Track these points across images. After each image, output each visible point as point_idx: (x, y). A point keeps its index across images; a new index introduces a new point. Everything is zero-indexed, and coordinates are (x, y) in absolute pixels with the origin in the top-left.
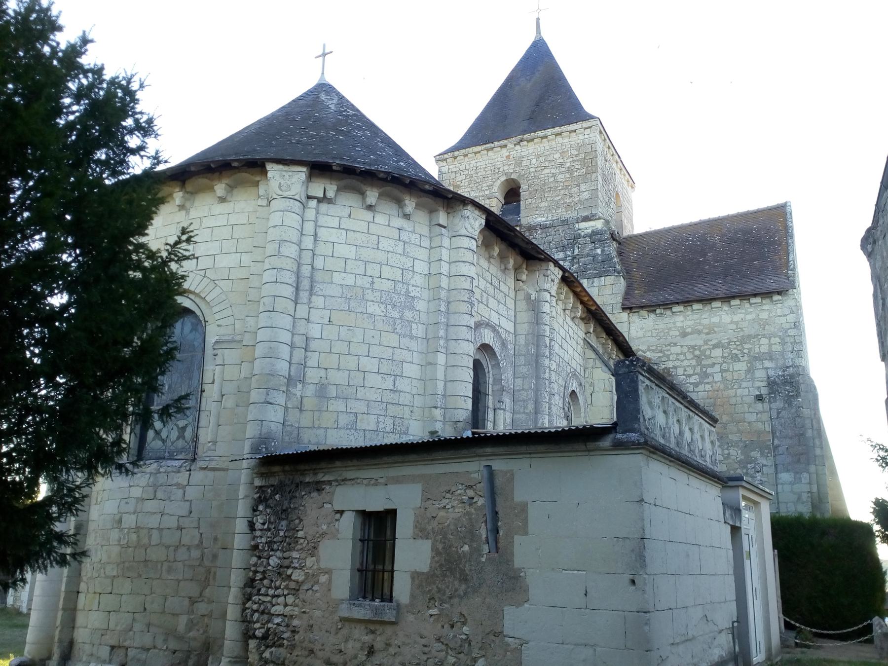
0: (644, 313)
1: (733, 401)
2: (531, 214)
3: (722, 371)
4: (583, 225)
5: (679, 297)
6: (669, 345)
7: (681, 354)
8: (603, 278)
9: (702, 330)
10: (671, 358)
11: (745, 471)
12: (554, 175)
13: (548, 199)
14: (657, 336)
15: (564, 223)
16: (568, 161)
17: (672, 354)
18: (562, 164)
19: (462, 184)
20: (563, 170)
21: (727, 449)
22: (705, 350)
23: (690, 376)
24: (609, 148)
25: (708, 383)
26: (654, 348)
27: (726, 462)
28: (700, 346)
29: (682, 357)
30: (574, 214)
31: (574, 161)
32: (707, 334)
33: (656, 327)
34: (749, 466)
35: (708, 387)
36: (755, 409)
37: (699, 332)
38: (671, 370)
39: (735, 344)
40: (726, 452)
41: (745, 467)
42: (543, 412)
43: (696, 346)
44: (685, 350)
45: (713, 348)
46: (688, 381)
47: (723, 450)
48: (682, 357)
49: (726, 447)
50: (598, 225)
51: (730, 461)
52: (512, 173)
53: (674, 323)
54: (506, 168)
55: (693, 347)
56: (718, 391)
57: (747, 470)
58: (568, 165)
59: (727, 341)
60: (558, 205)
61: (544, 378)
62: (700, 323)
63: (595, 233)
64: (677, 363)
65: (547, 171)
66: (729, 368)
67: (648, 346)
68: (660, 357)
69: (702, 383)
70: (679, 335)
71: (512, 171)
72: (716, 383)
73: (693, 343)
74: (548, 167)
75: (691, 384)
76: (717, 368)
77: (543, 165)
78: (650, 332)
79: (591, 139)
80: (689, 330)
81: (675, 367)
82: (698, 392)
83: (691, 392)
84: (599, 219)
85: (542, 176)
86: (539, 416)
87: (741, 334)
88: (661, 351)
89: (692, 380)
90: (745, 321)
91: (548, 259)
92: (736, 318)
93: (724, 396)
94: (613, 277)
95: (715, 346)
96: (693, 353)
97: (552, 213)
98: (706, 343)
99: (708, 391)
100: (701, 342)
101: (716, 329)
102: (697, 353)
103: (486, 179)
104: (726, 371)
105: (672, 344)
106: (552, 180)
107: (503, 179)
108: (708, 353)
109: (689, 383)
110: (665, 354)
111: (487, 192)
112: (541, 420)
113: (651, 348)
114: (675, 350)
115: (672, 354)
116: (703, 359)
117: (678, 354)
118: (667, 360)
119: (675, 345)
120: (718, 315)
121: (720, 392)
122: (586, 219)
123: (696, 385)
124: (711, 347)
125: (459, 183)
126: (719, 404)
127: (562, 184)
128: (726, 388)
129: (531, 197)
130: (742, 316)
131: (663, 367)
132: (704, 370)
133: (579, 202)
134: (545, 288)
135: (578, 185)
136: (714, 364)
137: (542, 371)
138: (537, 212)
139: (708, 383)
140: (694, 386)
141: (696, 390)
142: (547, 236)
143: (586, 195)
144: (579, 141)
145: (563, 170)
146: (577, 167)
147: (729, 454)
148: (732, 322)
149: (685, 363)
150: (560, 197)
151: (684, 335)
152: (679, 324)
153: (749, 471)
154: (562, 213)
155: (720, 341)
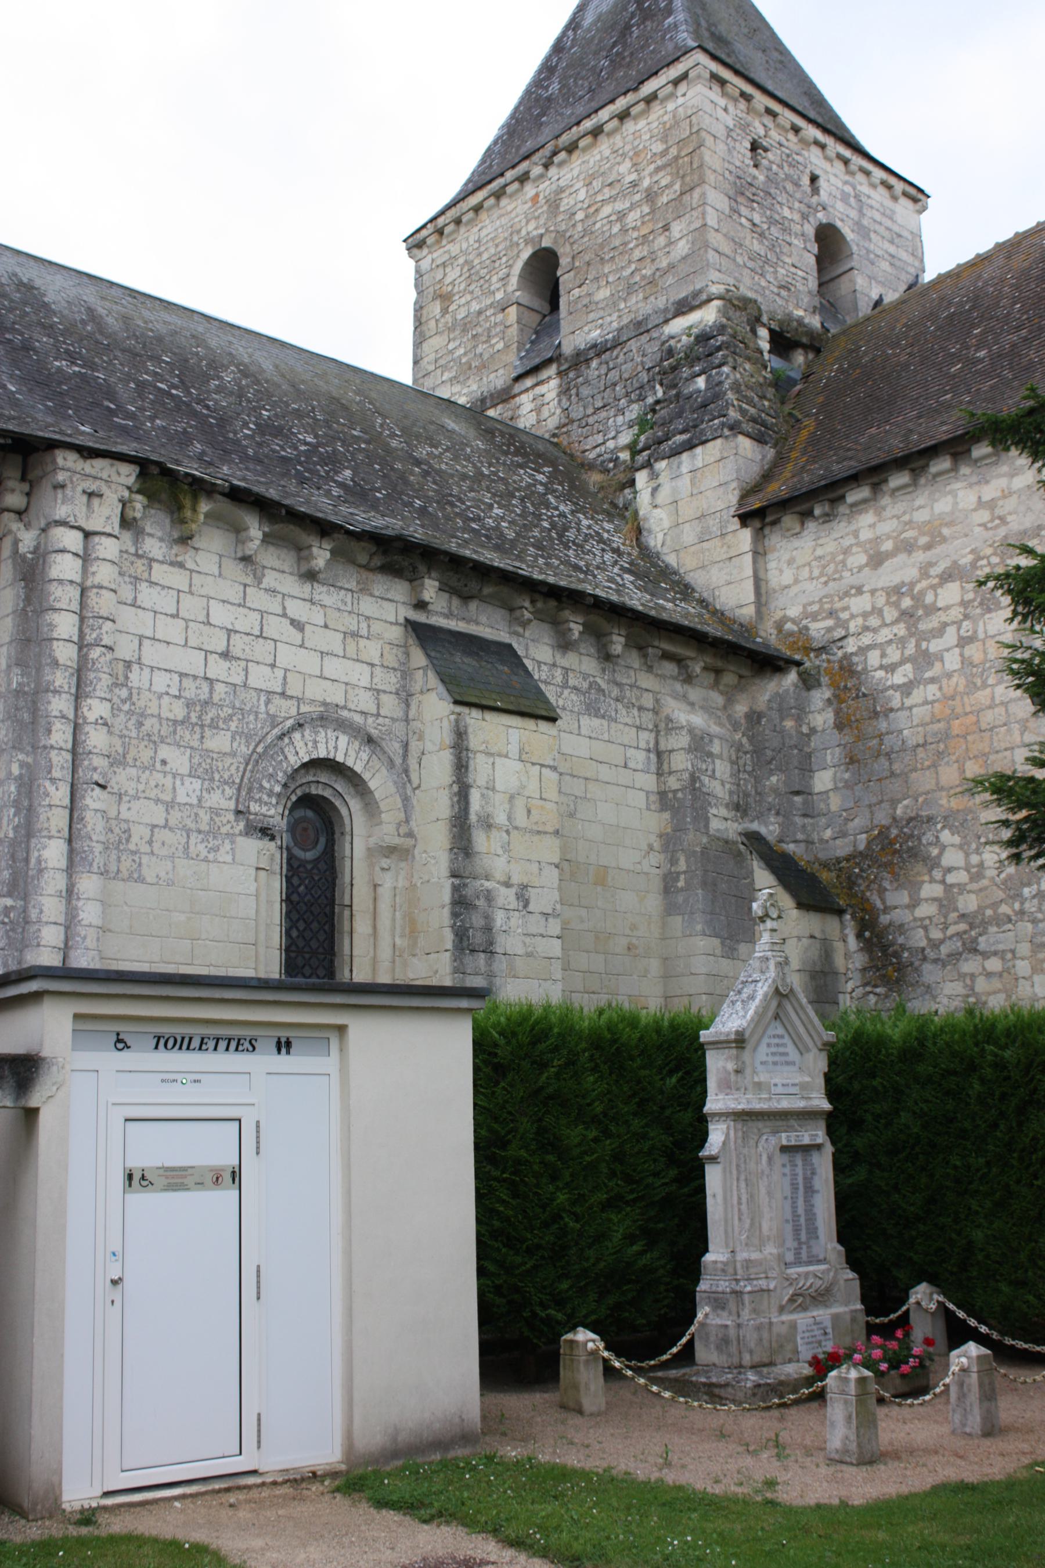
0: (789, 520)
1: (988, 718)
2: (579, 325)
3: (963, 642)
4: (678, 325)
5: (852, 466)
6: (847, 594)
7: (872, 613)
8: (699, 450)
9: (916, 539)
10: (853, 627)
11: (1017, 906)
12: (621, 216)
13: (610, 279)
14: (822, 575)
15: (641, 327)
16: (647, 172)
17: (853, 616)
18: (634, 184)
19: (456, 290)
20: (637, 197)
21: (978, 852)
22: (922, 593)
23: (891, 668)
24: (772, 114)
25: (932, 680)
26: (815, 608)
27: (974, 886)
28: (912, 585)
29: (874, 622)
30: (661, 302)
31: (658, 169)
32: (928, 547)
33: (819, 552)
34: (1026, 891)
35: (932, 688)
36: (1038, 734)
37: (907, 547)
38: (855, 659)
39: (989, 564)
40: (975, 859)
41: (1019, 896)
42: (40, 831)
43: (903, 584)
44: (881, 600)
45: (941, 585)
46: (889, 683)
47: (967, 855)
48: (874, 622)
49: (974, 846)
50: (708, 316)
51: (985, 882)
52: (541, 236)
53: (856, 534)
54: (531, 226)
55: (896, 591)
56: (952, 698)
57: (1022, 903)
58: (646, 183)
59: (970, 557)
60: (631, 289)
61: (45, 747)
62: (910, 522)
63: (703, 338)
64: (866, 639)
65: (607, 210)
66: (975, 632)
67: (804, 607)
68: (829, 630)
69: (919, 683)
70: (867, 565)
71: (542, 231)
72: (949, 675)
73: (896, 580)
74: (613, 199)
75: (895, 687)
76: (951, 636)
77: (599, 198)
78: (807, 568)
79: (690, 104)
80: (888, 546)
81: (863, 650)
82: (910, 708)
83: (898, 710)
84: (709, 300)
85: (598, 225)
86: (33, 841)
87: (1002, 532)
88: (831, 614)
89: (898, 678)
90: (1011, 494)
91: (52, 445)
92: (989, 492)
93: (968, 709)
94: (719, 441)
95: (946, 577)
96: (896, 605)
97: (619, 310)
98: (924, 574)
99: (932, 702)
100: (911, 573)
101: (946, 531)
102: (907, 603)
103: (497, 264)
104: (971, 639)
105: (853, 591)
106: (616, 229)
107: (526, 253)
108: (929, 598)
109: (892, 687)
110: (838, 618)
111: (499, 296)
112: (36, 854)
113: (809, 609)
114: (860, 604)
115: (853, 616)
116: (919, 618)
117: (865, 615)
118: (843, 633)
119: (860, 591)
120: (950, 492)
121: (958, 698)
122: (684, 307)
123: (906, 689)
124: (936, 581)
125: (450, 288)
126: (956, 732)
127: (635, 234)
128: (972, 687)
129: (578, 283)
130: (1003, 482)
131: (840, 653)
132: (924, 645)
133: (671, 267)
134: (57, 518)
135: (666, 228)
136: (945, 625)
137: (41, 731)
138: (592, 316)
139: (932, 680)
140: (902, 693)
141: (908, 702)
142: (609, 370)
143: (682, 248)
144: (666, 118)
145: (637, 197)
146: (663, 183)
147: (981, 865)
148: (981, 504)
149: (885, 635)
150: (633, 266)
151: (877, 560)
152: (865, 535)
153: (1027, 905)
154: (640, 306)
155: (955, 562)
